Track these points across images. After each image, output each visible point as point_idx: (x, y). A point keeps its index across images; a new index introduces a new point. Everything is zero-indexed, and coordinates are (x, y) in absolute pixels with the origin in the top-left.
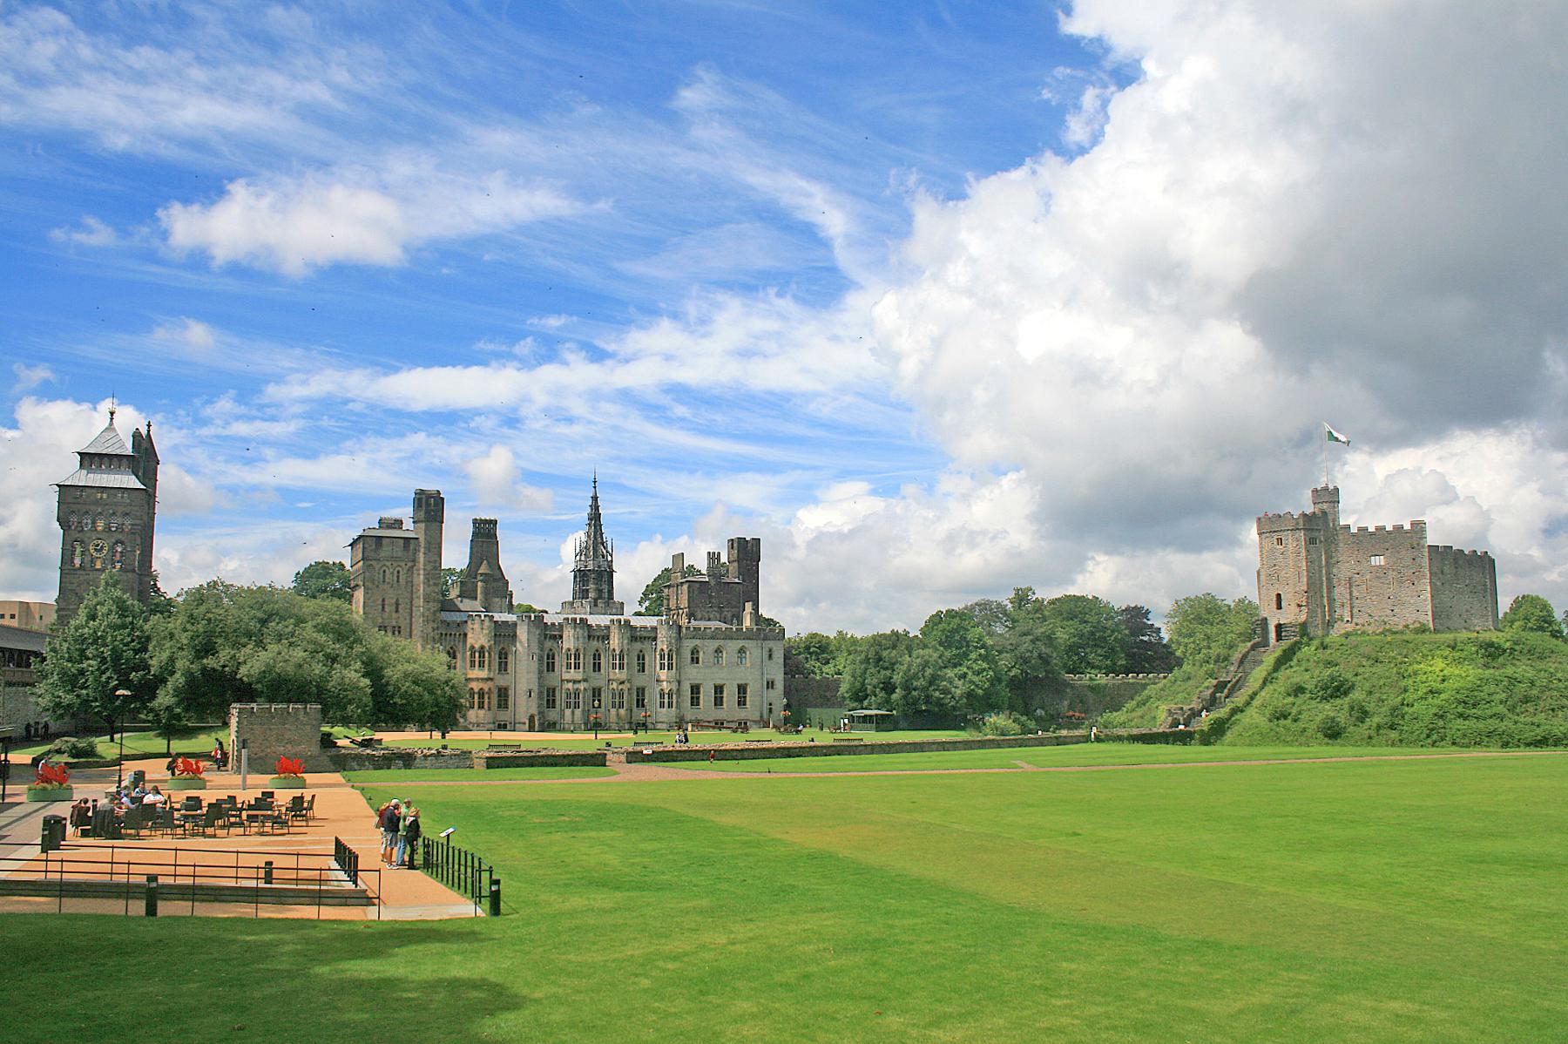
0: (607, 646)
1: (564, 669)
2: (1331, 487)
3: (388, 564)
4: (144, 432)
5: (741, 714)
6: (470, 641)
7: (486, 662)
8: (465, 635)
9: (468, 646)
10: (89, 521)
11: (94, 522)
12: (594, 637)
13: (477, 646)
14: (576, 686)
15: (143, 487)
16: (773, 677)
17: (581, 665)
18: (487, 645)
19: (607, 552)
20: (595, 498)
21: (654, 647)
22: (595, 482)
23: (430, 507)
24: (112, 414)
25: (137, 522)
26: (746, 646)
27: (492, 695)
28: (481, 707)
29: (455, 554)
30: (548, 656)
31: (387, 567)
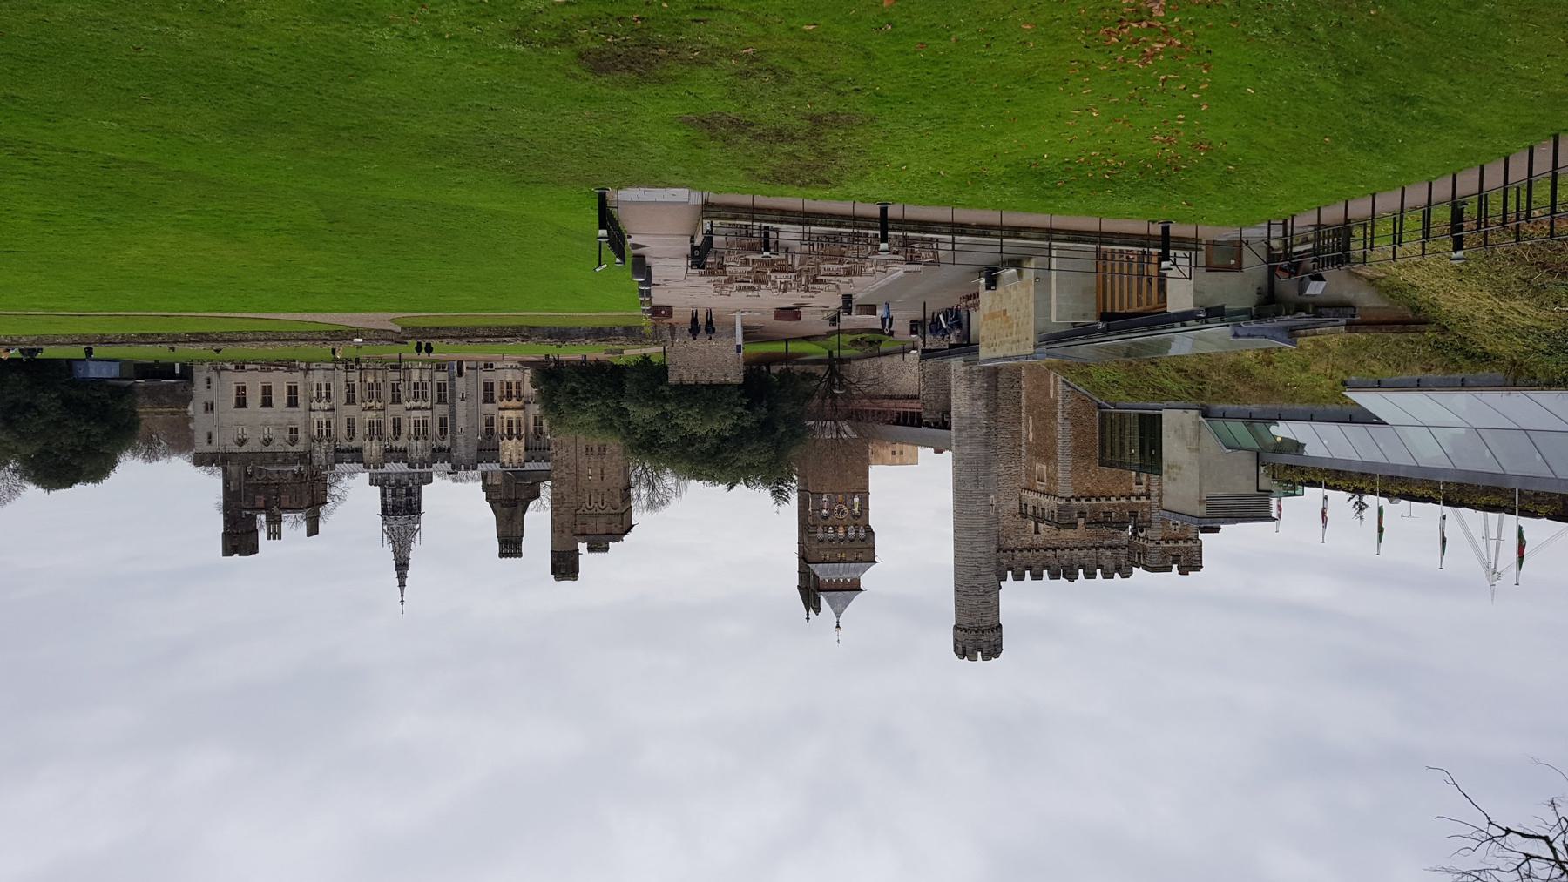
0: (386, 443)
1: (429, 420)
4: (812, 612)
5: (241, 377)
6: (522, 443)
7: (506, 424)
8: (526, 449)
9: (523, 439)
10: (850, 534)
11: (846, 533)
12: (400, 451)
13: (515, 439)
15: (810, 565)
16: (206, 415)
17: (412, 424)
19: (387, 533)
20: (402, 585)
21: (338, 443)
22: (402, 601)
23: (564, 566)
24: (838, 626)
25: (812, 535)
26: (237, 447)
27: (499, 394)
28: (509, 385)
29: (538, 521)
30: (446, 432)
31: (600, 508)
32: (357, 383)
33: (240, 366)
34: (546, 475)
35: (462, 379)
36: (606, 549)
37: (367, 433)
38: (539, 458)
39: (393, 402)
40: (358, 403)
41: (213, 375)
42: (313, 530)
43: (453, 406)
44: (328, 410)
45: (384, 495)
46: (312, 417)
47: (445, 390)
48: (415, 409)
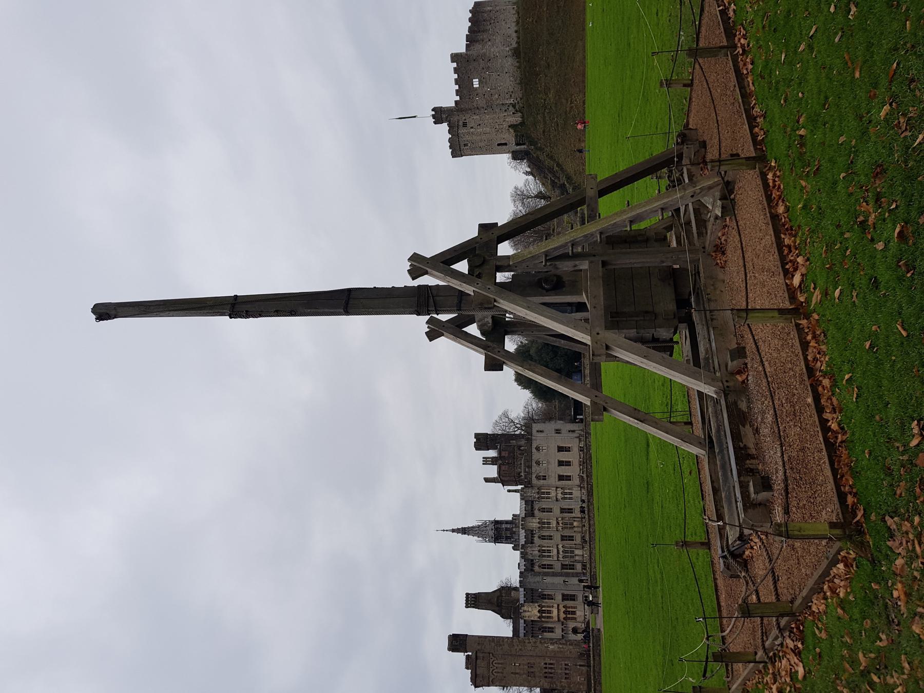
1: (551, 559)
2: (433, 113)
3: (491, 669)
5: (576, 450)
6: (536, 619)
7: (548, 609)
8: (532, 621)
12: (532, 540)
13: (539, 615)
14: (561, 553)
18: (538, 608)
20: (453, 531)
22: (444, 530)
23: (457, 643)
28: (574, 613)
30: (543, 568)
32: (573, 515)
33: (581, 449)
34: (516, 631)
35: (577, 582)
36: (467, 668)
37: (543, 521)
38: (527, 630)
39: (562, 536)
40: (562, 515)
41: (576, 435)
42: (487, 480)
43: (561, 575)
44: (557, 498)
45: (507, 522)
46: (553, 489)
47: (570, 569)
48: (558, 550)
